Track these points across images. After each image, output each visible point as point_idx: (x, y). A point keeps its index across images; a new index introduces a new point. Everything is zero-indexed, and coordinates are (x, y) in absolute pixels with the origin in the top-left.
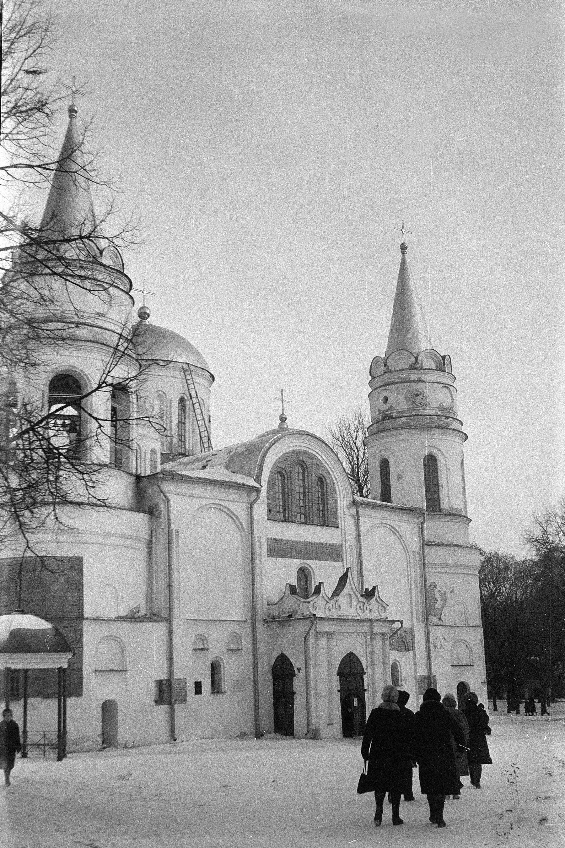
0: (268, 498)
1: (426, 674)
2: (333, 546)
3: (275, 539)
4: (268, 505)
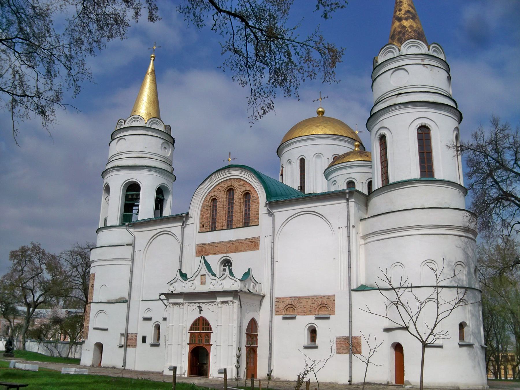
0: (202, 218)
1: (347, 335)
2: (252, 239)
3: (204, 244)
4: (201, 223)
